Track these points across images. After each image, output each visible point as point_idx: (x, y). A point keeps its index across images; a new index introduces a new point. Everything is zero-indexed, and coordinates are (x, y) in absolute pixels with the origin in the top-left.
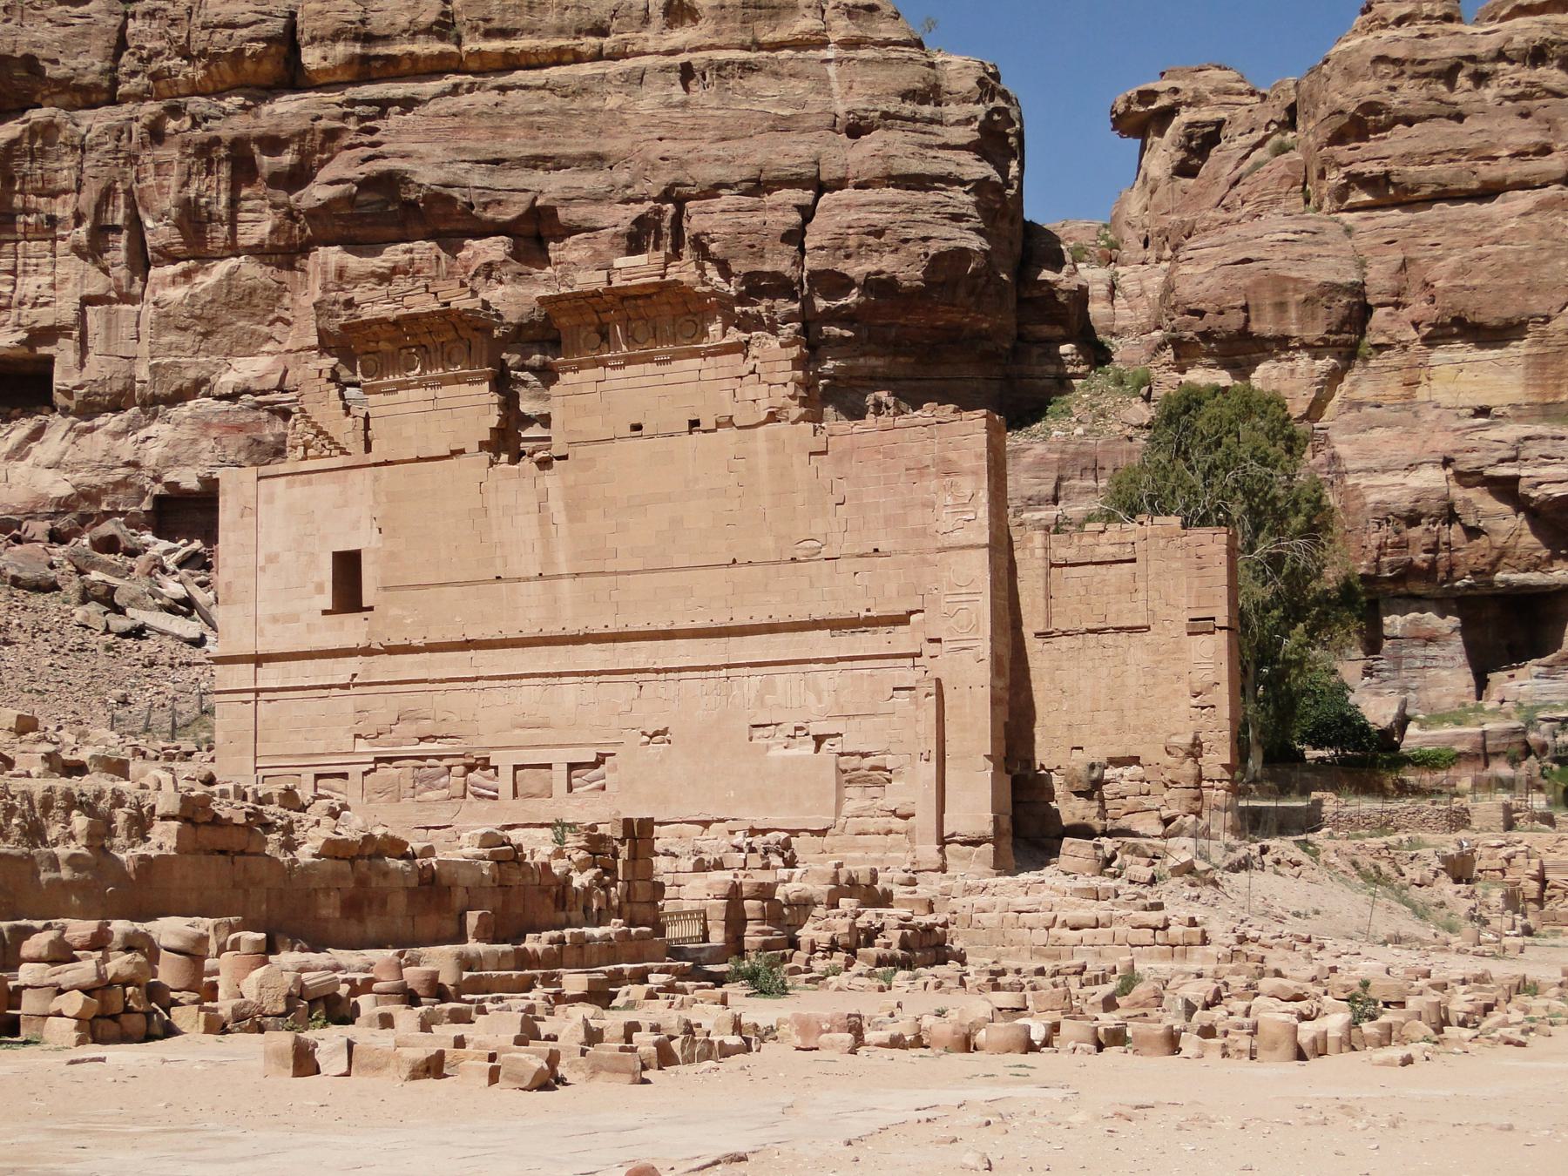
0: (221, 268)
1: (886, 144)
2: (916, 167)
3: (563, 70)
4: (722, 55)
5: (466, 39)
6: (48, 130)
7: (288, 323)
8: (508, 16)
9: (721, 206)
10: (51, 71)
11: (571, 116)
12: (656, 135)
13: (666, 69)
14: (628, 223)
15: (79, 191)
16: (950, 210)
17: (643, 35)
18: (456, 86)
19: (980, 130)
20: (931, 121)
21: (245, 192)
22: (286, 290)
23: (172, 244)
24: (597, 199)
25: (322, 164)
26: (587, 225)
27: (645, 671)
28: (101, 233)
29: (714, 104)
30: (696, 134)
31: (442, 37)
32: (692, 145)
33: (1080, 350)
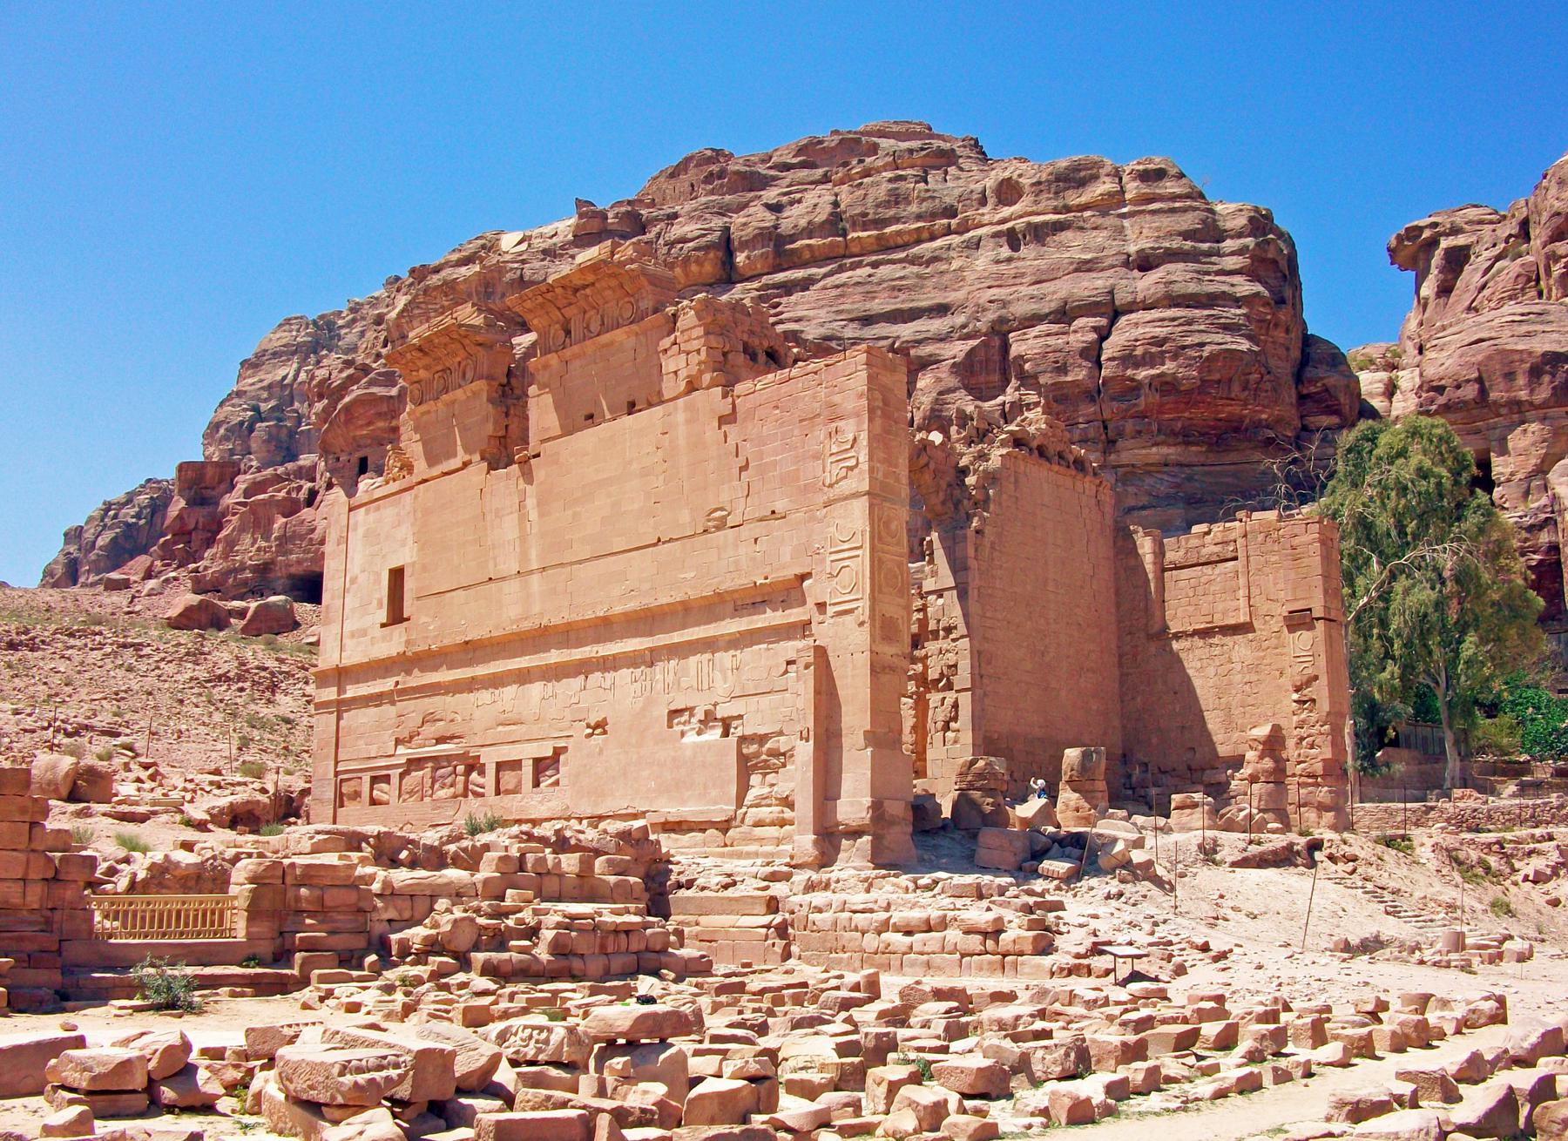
2: (1193, 288)
13: (996, 235)
24: (942, 339)
30: (1018, 281)
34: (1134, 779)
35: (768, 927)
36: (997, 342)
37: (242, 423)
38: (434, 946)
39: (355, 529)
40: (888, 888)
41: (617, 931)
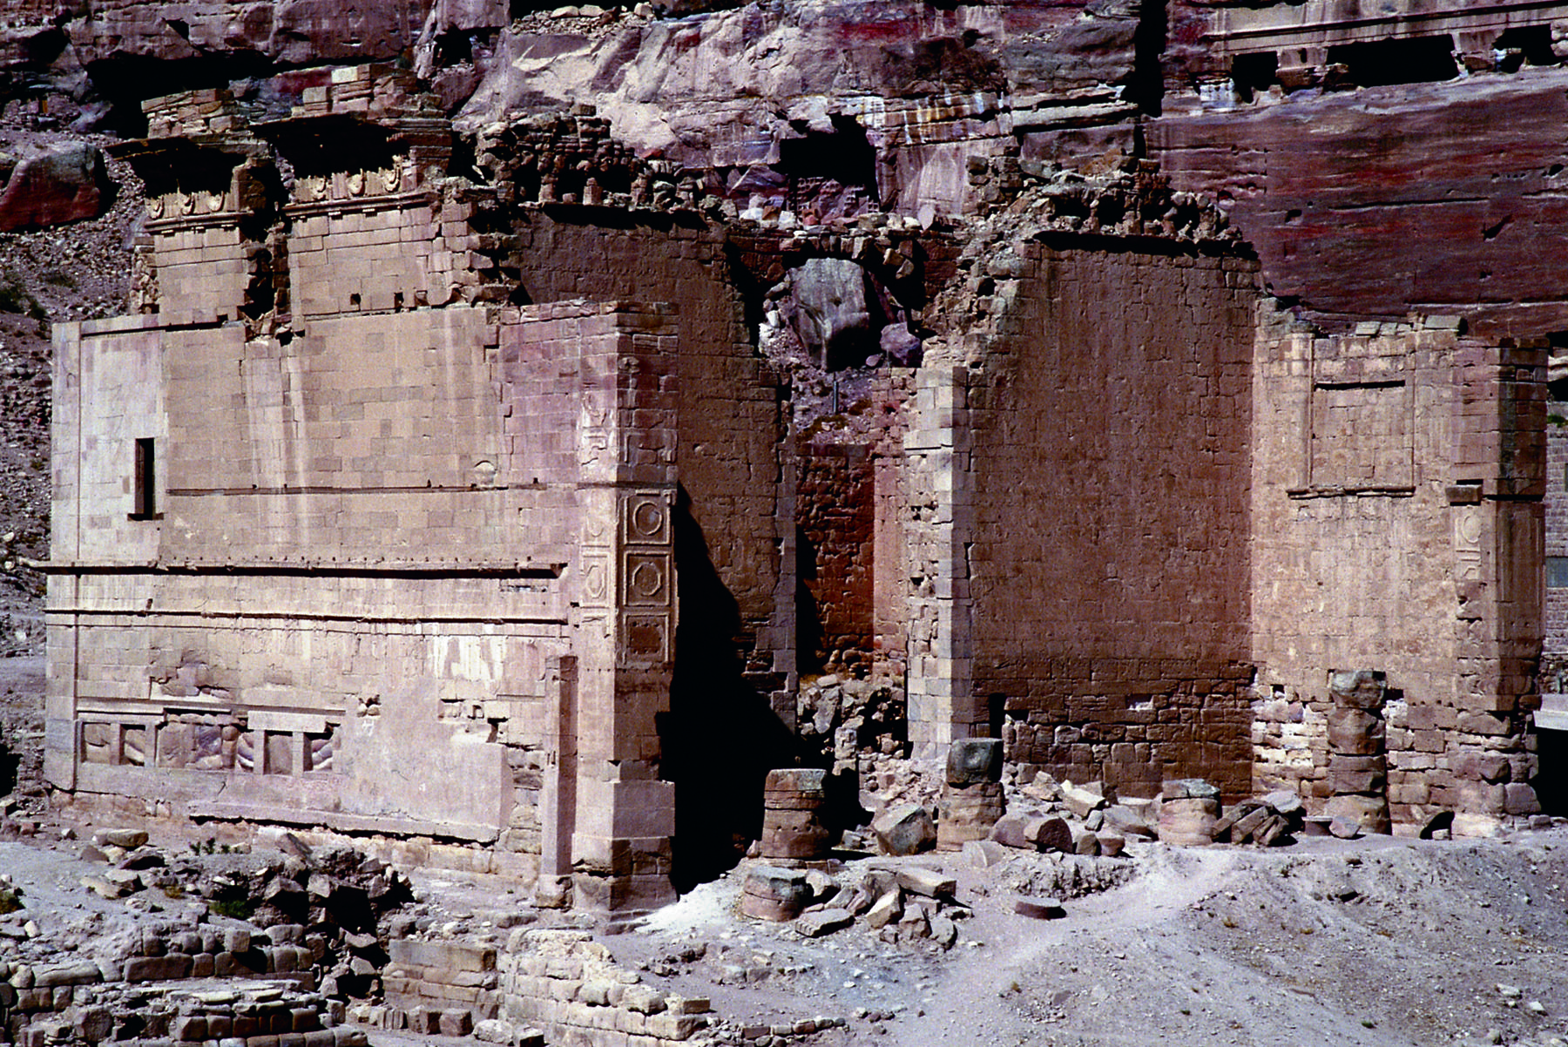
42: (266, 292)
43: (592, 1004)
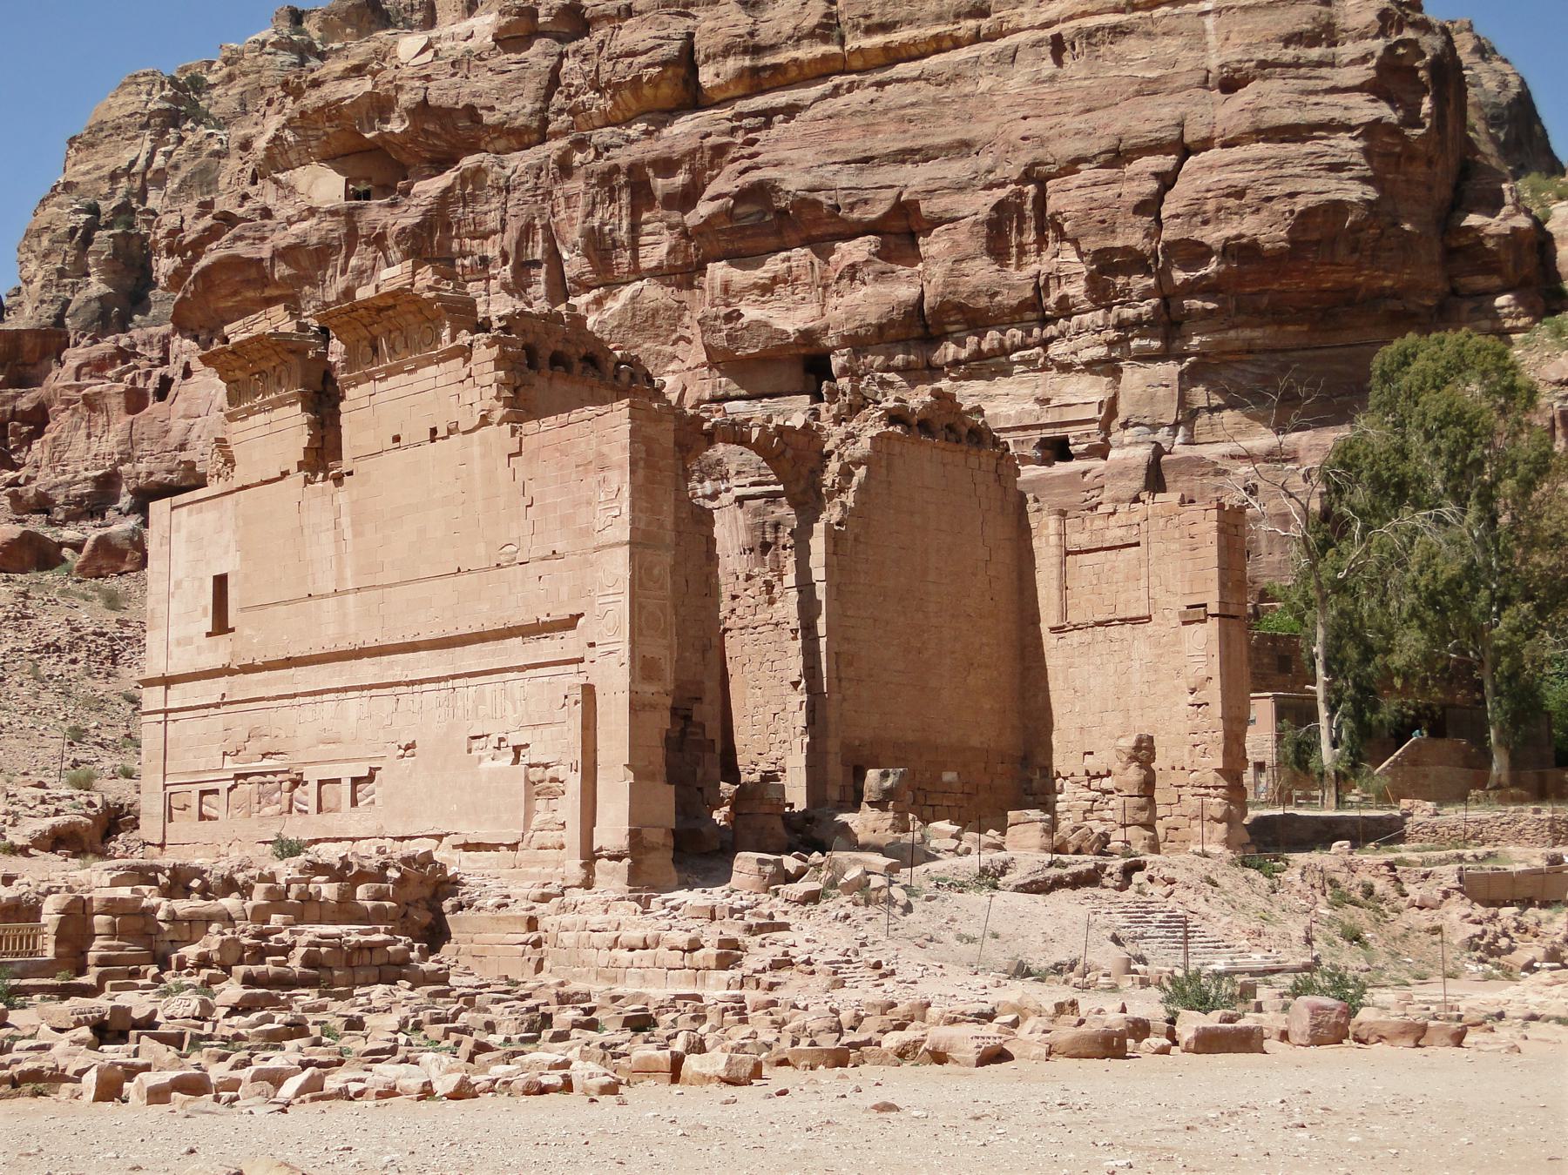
0: (626, 292)
1: (1260, 95)
2: (1290, 116)
3: (942, 57)
4: (1090, 22)
5: (848, 37)
6: (479, 171)
7: (689, 342)
8: (888, 9)
9: (1077, 183)
10: (489, 118)
11: (944, 104)
12: (1020, 115)
13: (1036, 44)
14: (987, 209)
15: (503, 230)
16: (1327, 160)
17: (1018, 11)
18: (837, 87)
19: (1377, 67)
20: (1320, 64)
21: (645, 216)
22: (685, 309)
23: (583, 274)
24: (960, 188)
25: (712, 178)
26: (948, 216)
27: (398, 684)
28: (524, 268)
29: (1082, 75)
30: (1061, 109)
31: (826, 40)
32: (1055, 120)
33: (1519, 301)
34: (1035, 784)
35: (526, 943)
36: (1031, 189)
37: (73, 231)
38: (204, 961)
39: (178, 531)
40: (622, 910)
41: (360, 947)
42: (323, 454)
43: (632, 950)
